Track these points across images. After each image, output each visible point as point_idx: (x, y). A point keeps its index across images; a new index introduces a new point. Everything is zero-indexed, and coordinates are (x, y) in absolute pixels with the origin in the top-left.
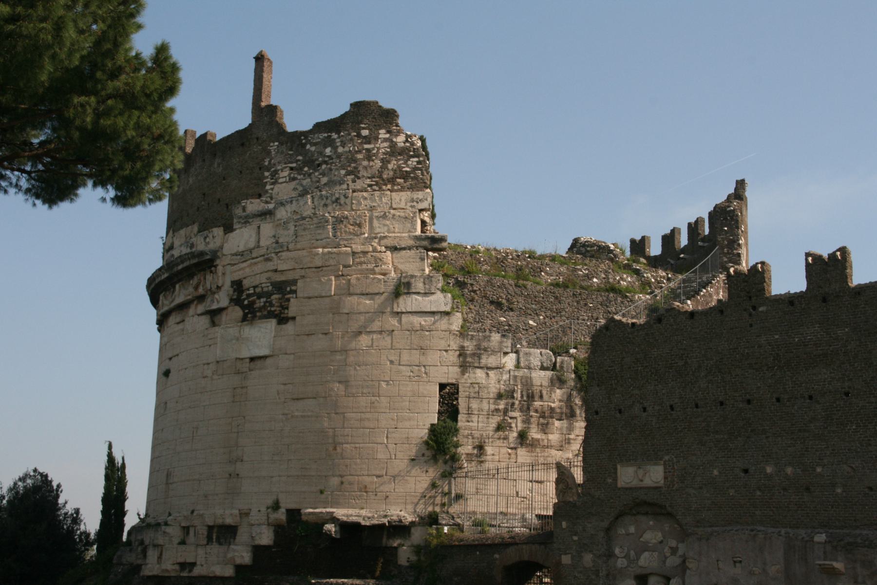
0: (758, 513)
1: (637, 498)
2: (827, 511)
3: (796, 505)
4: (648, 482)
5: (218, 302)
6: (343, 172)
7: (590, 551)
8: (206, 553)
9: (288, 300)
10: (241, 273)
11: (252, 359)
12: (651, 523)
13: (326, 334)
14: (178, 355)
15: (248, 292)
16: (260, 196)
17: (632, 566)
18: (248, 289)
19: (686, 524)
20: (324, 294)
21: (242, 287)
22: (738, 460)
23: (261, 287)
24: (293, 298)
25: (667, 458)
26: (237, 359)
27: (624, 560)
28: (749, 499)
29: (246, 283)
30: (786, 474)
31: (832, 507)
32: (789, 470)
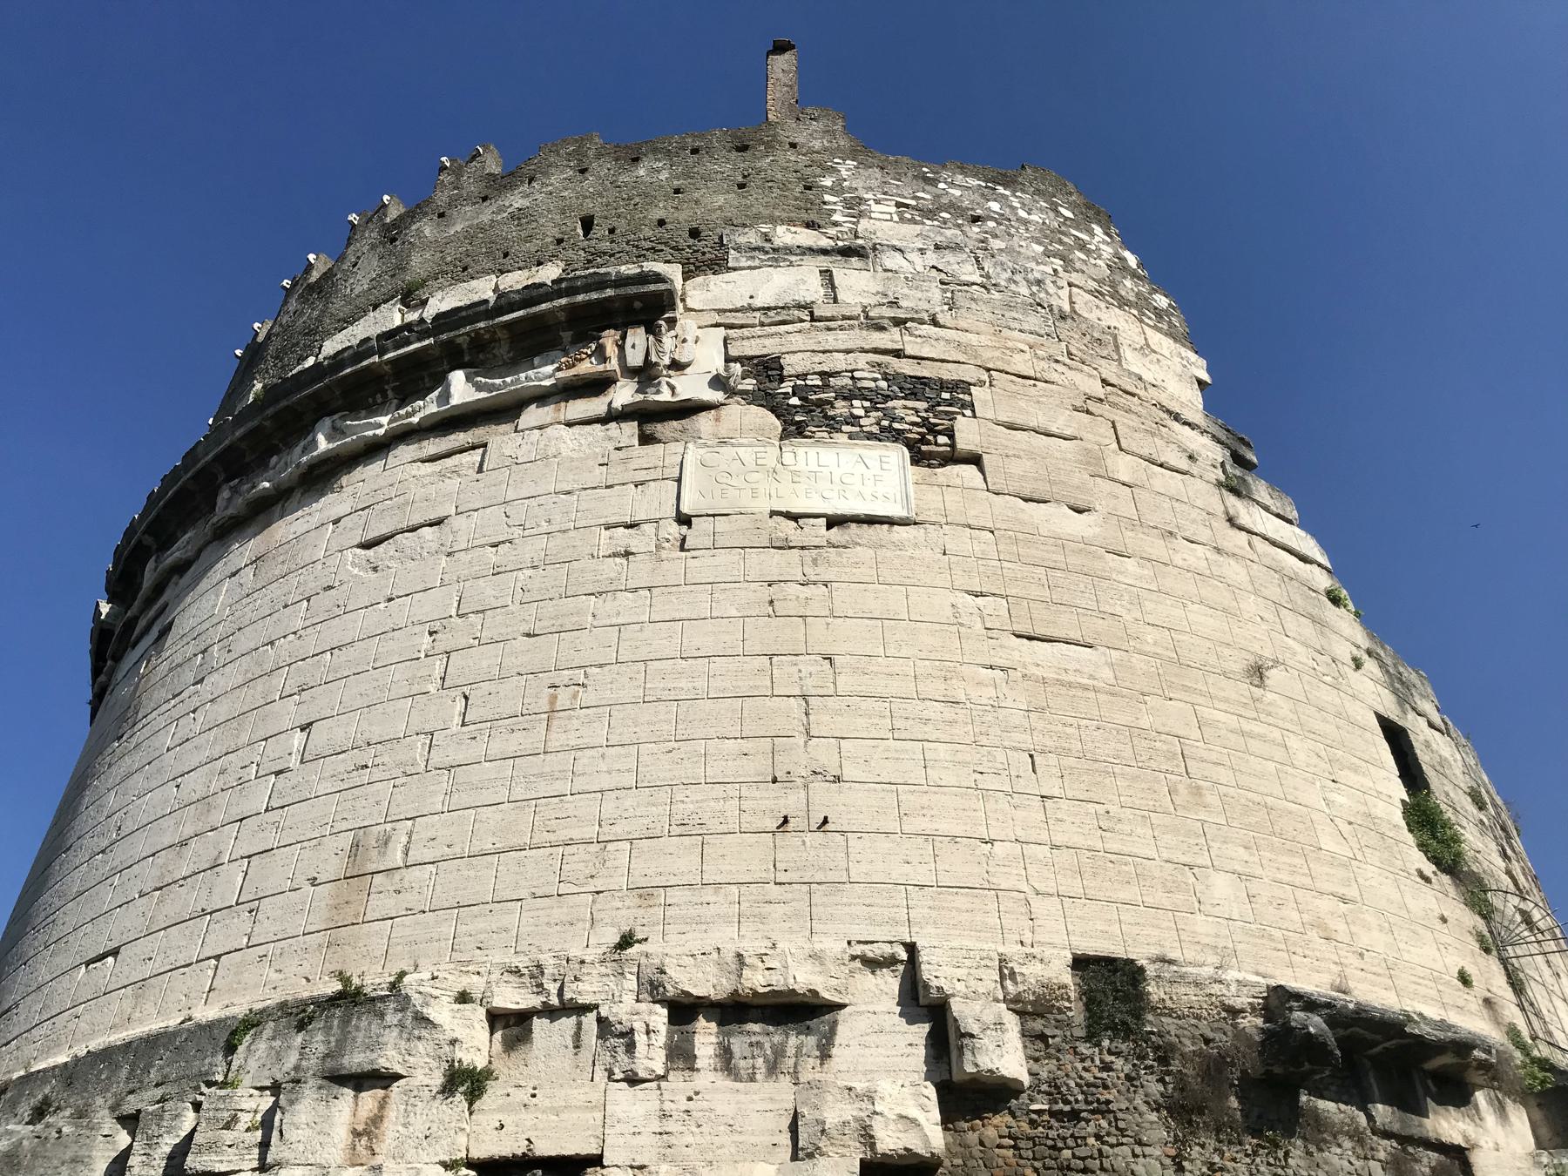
5: (673, 388)
6: (1041, 249)
8: (664, 1116)
9: (951, 417)
10: (767, 342)
11: (834, 522)
13: (1079, 511)
14: (438, 523)
15: (799, 382)
16: (810, 225)
18: (803, 376)
20: (1054, 430)
21: (782, 368)
23: (853, 378)
24: (964, 415)
26: (773, 513)
29: (793, 364)
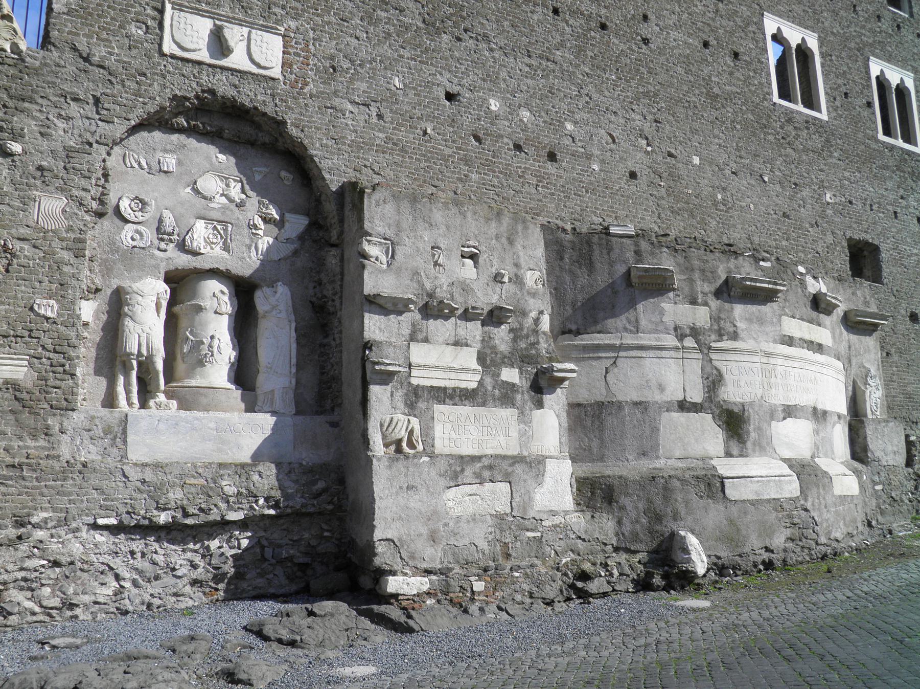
0: (474, 176)
1: (212, 92)
2: (579, 196)
3: (536, 176)
4: (238, 59)
7: (62, 190)
12: (222, 157)
17: (163, 245)
19: (330, 169)
22: (441, 74)
25: (293, 24)
27: (140, 228)
28: (460, 148)
30: (521, 120)
31: (587, 191)
32: (526, 115)
